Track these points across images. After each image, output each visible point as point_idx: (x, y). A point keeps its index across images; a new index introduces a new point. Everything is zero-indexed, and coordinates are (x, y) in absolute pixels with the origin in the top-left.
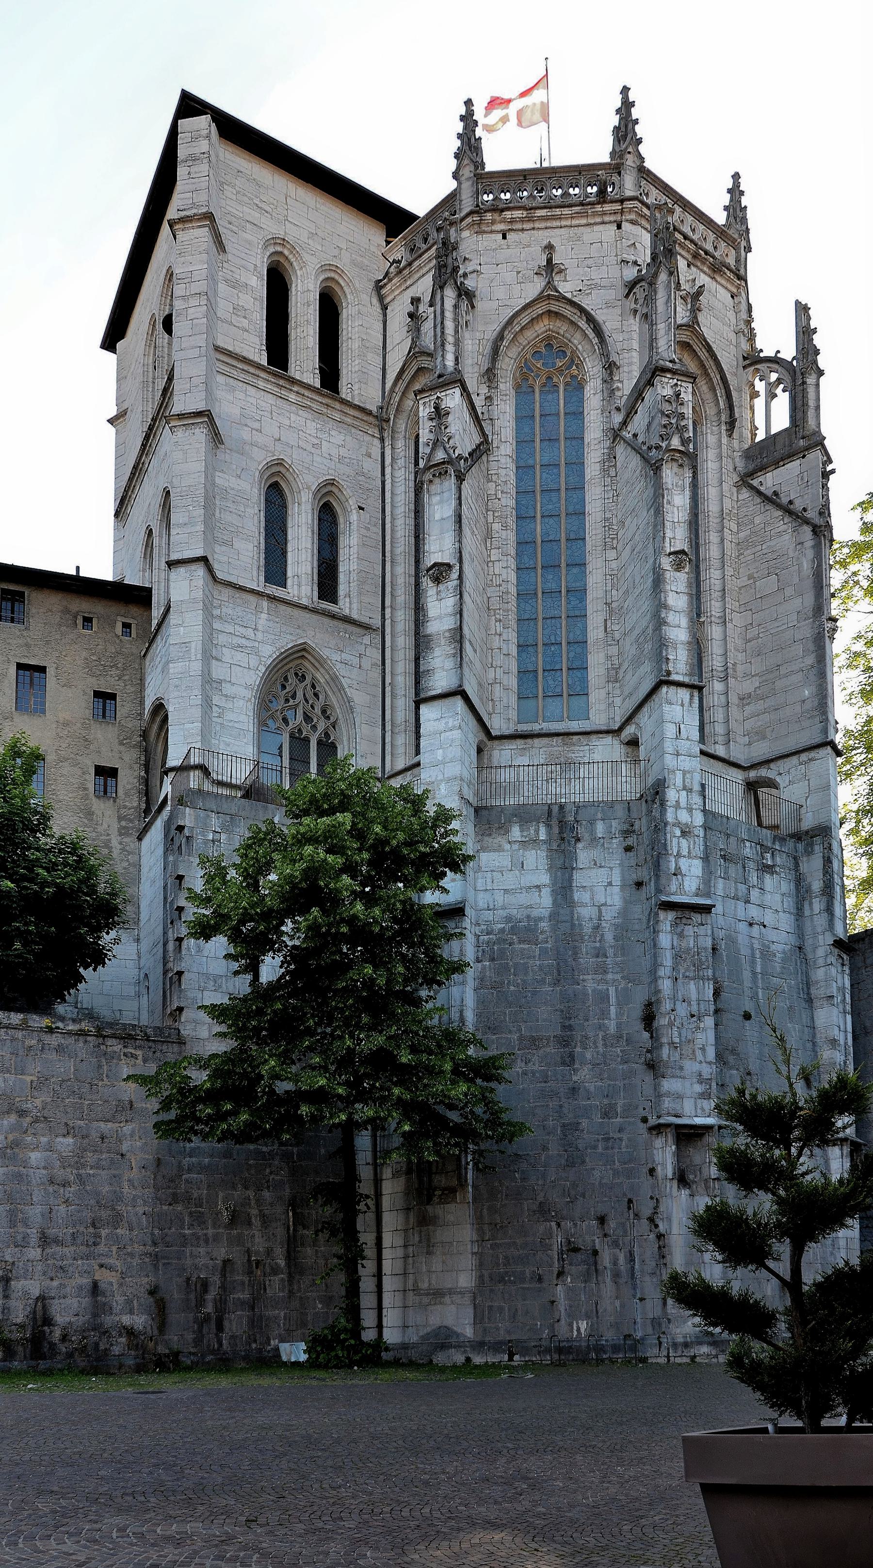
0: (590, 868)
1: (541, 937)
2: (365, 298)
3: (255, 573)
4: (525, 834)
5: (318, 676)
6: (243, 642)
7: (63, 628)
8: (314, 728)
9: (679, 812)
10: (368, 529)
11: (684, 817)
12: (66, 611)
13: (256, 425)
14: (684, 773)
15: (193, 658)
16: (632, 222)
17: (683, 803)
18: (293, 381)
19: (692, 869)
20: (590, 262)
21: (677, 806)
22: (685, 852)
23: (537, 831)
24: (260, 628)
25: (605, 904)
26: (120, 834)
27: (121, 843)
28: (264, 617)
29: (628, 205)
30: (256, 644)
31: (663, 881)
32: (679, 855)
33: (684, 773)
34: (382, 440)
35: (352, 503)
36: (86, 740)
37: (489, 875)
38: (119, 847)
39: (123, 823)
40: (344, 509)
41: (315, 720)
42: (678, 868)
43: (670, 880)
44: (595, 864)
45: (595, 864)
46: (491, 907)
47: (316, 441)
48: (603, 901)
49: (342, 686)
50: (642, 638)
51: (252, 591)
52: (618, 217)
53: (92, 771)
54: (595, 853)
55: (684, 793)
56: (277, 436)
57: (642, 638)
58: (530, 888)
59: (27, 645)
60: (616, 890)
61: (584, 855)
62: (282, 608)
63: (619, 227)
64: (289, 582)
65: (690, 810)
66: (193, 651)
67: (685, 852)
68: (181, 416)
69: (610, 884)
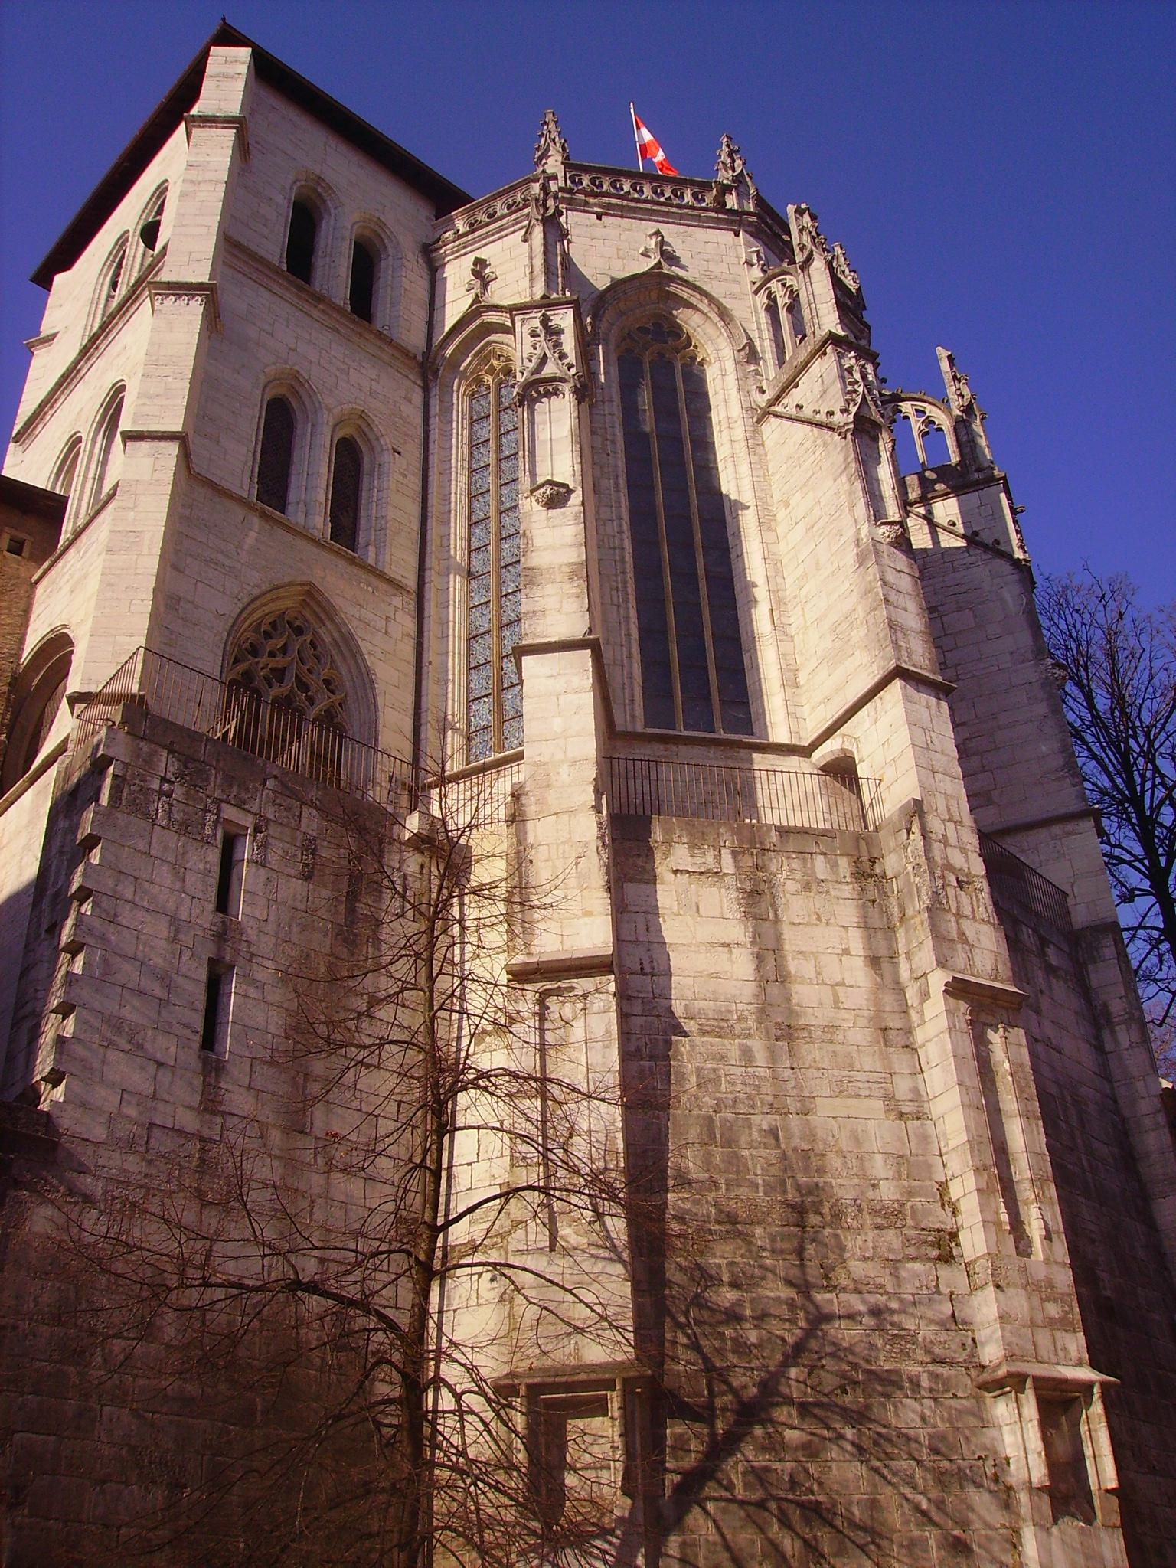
0: (808, 924)
1: (738, 1028)
2: (410, 256)
3: (247, 481)
4: (699, 860)
5: (322, 631)
6: (221, 557)
8: (311, 701)
9: (949, 850)
10: (405, 476)
11: (957, 859)
13: (268, 328)
15: (145, 551)
17: (952, 840)
18: (319, 299)
19: (982, 938)
20: (706, 257)
22: (967, 911)
23: (719, 857)
24: (246, 547)
25: (842, 984)
28: (254, 533)
30: (239, 566)
32: (959, 915)
34: (426, 390)
35: (387, 442)
37: (640, 918)
40: (372, 449)
41: (313, 688)
42: (962, 934)
44: (819, 919)
45: (819, 919)
46: (648, 970)
47: (342, 366)
48: (838, 979)
49: (359, 650)
50: (845, 625)
51: (239, 500)
54: (816, 902)
55: (951, 826)
56: (293, 346)
57: (845, 625)
58: (712, 945)
60: (859, 962)
61: (793, 903)
62: (280, 532)
63: (737, 235)
64: (290, 509)
65: (963, 851)
66: (146, 542)
67: (967, 911)
68: (170, 285)
69: (846, 952)
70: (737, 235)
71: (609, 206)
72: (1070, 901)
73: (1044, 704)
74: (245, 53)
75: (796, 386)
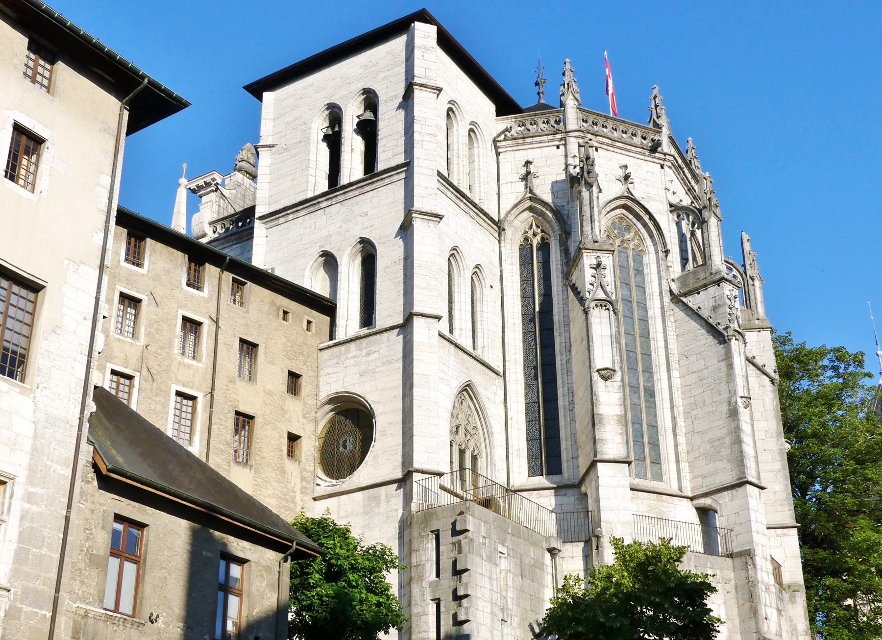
7: (271, 317)
11: (766, 579)
12: (273, 303)
14: (763, 546)
16: (670, 167)
17: (764, 569)
21: (762, 569)
22: (768, 603)
26: (302, 493)
27: (302, 500)
29: (667, 157)
31: (760, 623)
32: (765, 605)
33: (763, 546)
36: (282, 410)
38: (301, 503)
39: (304, 484)
43: (763, 622)
52: (662, 162)
53: (286, 436)
59: (247, 325)
65: (767, 572)
70: (662, 167)
71: (602, 143)
72: (783, 569)
73: (779, 463)
74: (432, 30)
75: (698, 293)
